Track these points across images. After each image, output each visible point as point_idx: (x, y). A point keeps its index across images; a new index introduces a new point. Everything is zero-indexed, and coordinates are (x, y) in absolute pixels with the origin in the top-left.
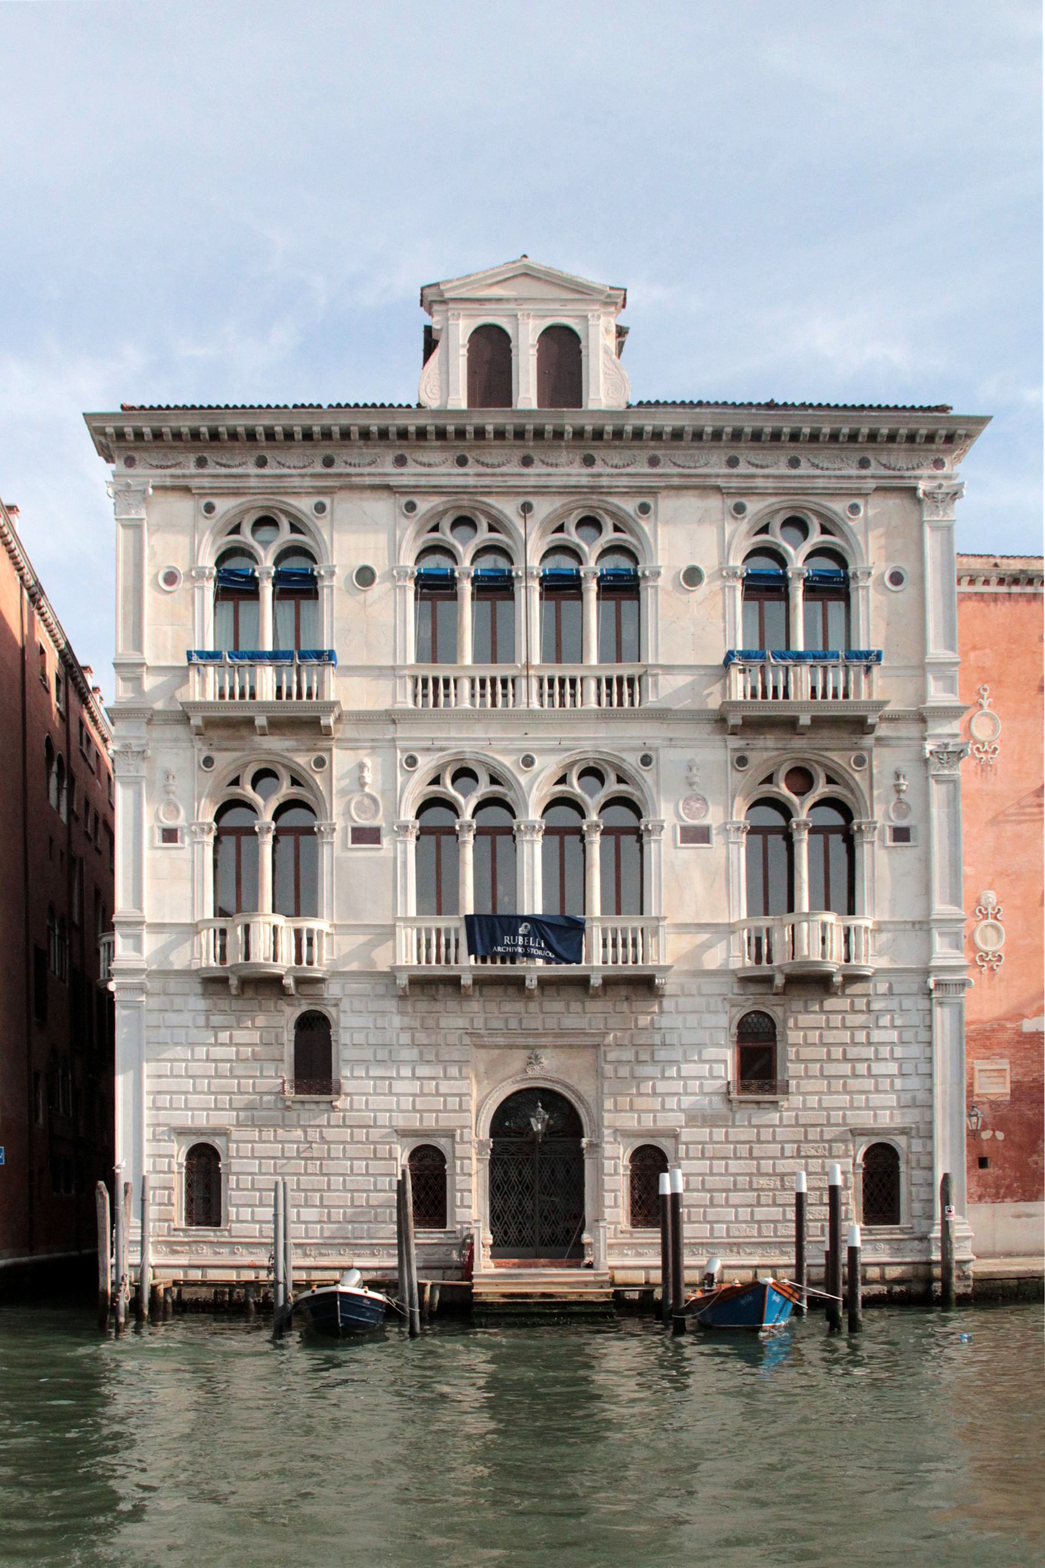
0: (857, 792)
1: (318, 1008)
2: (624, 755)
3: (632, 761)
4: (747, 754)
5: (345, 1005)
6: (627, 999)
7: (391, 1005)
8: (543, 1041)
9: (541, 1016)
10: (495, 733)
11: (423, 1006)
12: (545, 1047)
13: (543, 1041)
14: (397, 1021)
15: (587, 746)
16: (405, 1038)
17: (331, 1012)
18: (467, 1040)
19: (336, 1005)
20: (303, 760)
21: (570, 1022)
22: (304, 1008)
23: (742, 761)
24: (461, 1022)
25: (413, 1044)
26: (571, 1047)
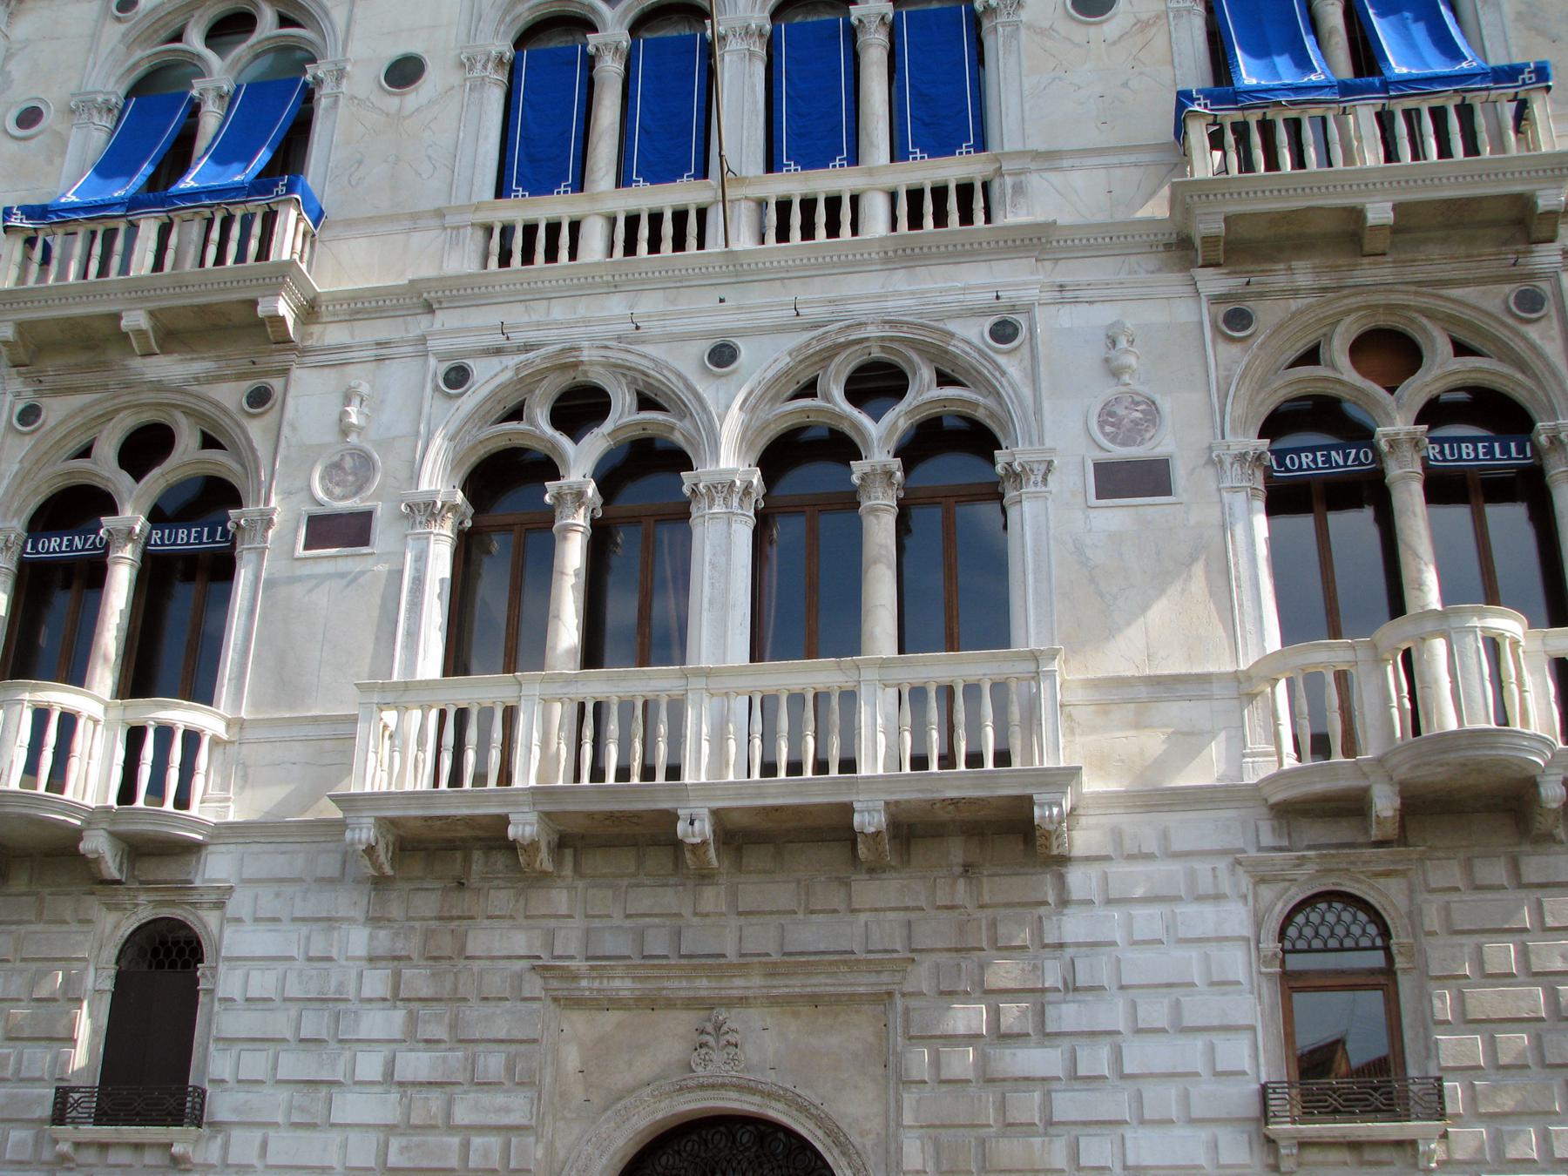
0: (1537, 366)
1: (178, 913)
2: (951, 326)
3: (971, 334)
4: (1249, 305)
5: (232, 908)
6: (967, 868)
7: (349, 902)
8: (737, 985)
9: (734, 921)
10: (650, 304)
11: (427, 903)
12: (743, 1001)
13: (737, 985)
14: (358, 939)
15: (860, 309)
16: (376, 982)
17: (207, 922)
18: (534, 985)
19: (220, 905)
20: (231, 395)
21: (812, 934)
22: (145, 914)
23: (1237, 319)
24: (519, 941)
25: (396, 997)
26: (815, 1000)
